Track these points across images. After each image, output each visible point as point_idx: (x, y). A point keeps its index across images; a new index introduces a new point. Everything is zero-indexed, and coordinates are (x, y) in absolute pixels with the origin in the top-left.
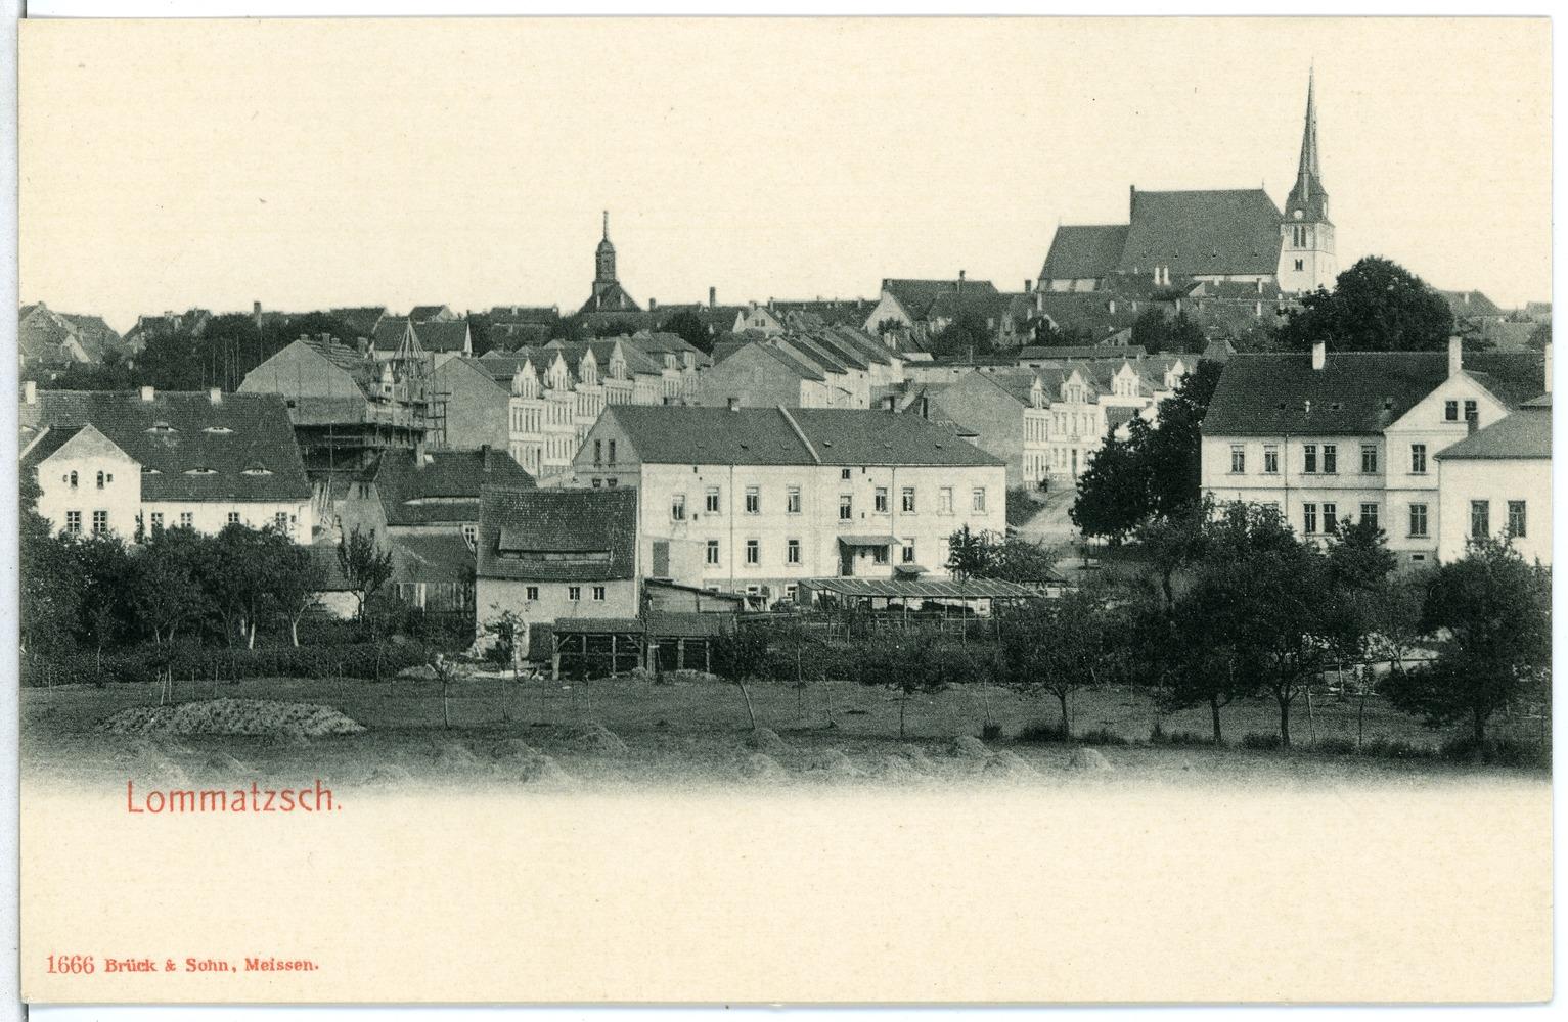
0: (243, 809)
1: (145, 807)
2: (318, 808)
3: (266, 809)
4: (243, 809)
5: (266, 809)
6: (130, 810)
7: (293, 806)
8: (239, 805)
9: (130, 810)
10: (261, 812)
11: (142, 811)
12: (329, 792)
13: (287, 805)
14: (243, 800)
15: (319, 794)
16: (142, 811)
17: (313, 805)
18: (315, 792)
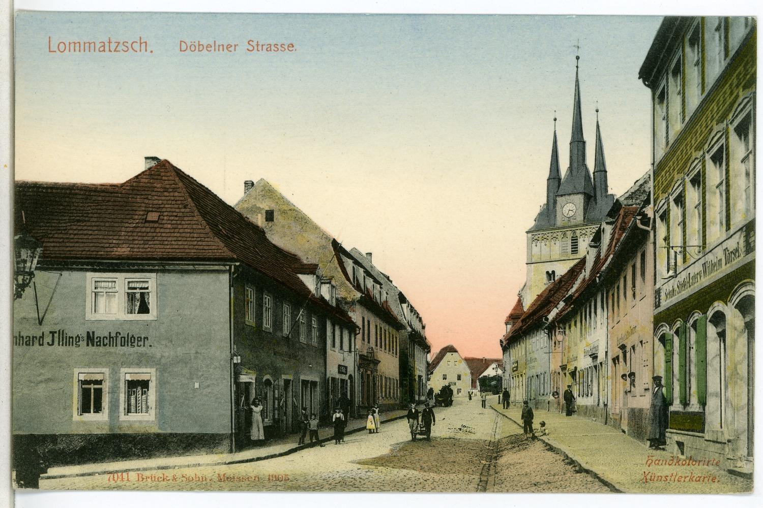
0: (104, 51)
1: (57, 50)
2: (140, 51)
3: (115, 51)
4: (104, 51)
5: (115, 51)
6: (50, 51)
7: (128, 49)
8: (102, 49)
9: (50, 51)
10: (113, 53)
11: (55, 51)
12: (146, 42)
13: (125, 49)
14: (104, 46)
15: (141, 43)
16: (55, 51)
17: (138, 49)
18: (139, 42)
